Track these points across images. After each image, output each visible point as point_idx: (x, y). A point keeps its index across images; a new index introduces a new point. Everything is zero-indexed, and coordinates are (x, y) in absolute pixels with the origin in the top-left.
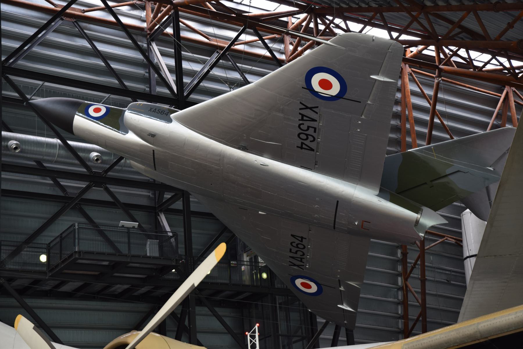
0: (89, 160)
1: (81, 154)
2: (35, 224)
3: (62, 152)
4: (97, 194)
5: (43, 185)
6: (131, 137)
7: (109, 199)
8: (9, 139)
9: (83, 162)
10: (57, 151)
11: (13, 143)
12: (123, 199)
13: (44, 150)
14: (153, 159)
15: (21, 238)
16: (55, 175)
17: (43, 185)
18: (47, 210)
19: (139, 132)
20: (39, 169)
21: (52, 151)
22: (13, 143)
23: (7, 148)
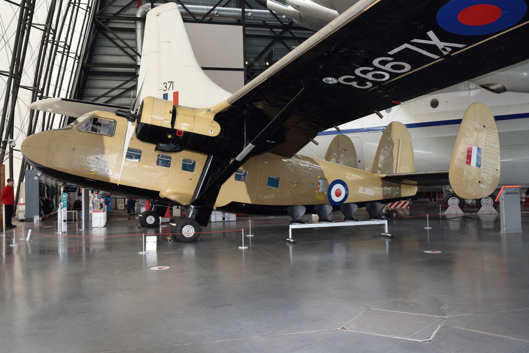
0: (282, 19)
1: (279, 16)
2: (262, 49)
3: (272, 16)
4: (288, 35)
5: (266, 32)
6: (290, 8)
7: (291, 36)
8: (248, 12)
9: (279, 20)
10: (268, 16)
11: (249, 14)
12: (297, 36)
13: (263, 16)
14: (300, 18)
15: (256, 55)
16: (271, 27)
17: (266, 32)
18: (267, 42)
19: (294, 6)
20: (265, 25)
21: (266, 16)
22: (249, 14)
23: (247, 16)
